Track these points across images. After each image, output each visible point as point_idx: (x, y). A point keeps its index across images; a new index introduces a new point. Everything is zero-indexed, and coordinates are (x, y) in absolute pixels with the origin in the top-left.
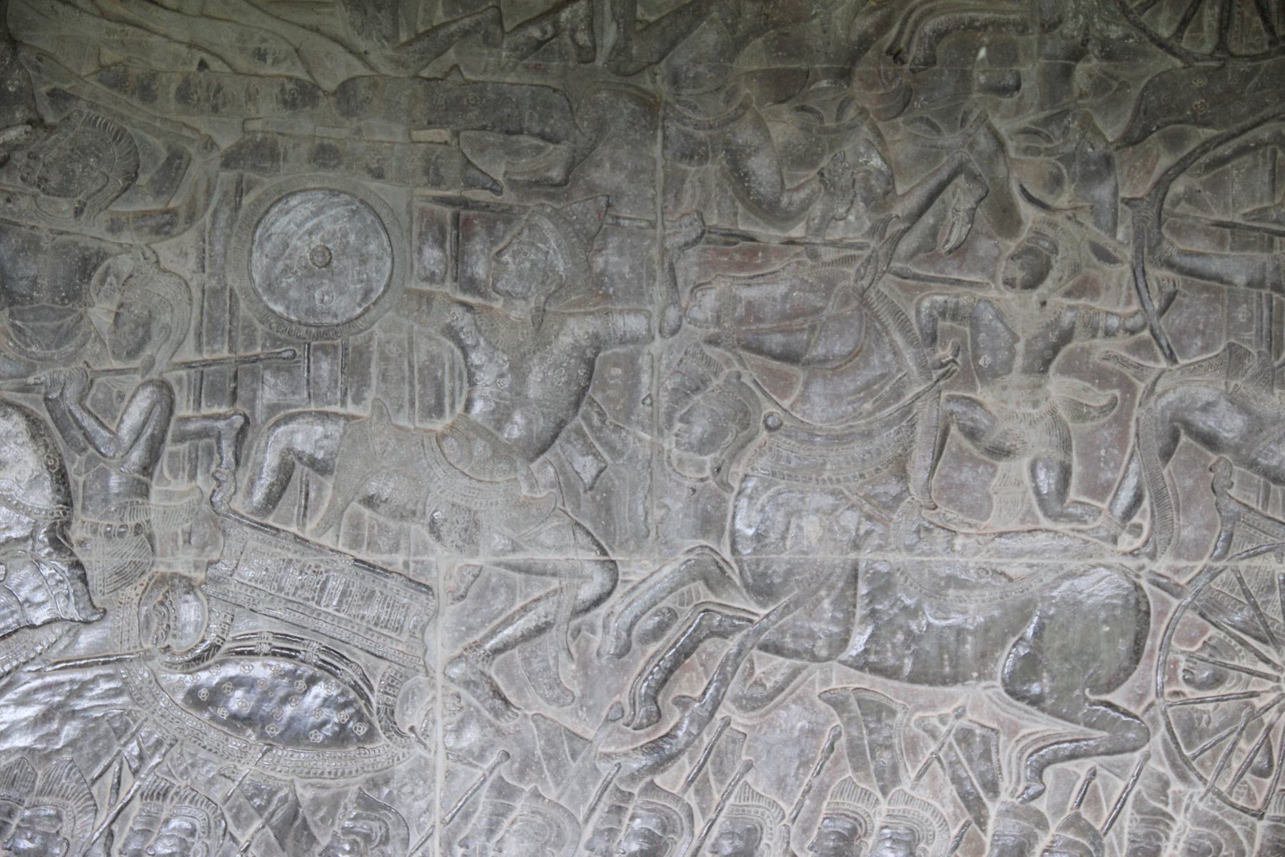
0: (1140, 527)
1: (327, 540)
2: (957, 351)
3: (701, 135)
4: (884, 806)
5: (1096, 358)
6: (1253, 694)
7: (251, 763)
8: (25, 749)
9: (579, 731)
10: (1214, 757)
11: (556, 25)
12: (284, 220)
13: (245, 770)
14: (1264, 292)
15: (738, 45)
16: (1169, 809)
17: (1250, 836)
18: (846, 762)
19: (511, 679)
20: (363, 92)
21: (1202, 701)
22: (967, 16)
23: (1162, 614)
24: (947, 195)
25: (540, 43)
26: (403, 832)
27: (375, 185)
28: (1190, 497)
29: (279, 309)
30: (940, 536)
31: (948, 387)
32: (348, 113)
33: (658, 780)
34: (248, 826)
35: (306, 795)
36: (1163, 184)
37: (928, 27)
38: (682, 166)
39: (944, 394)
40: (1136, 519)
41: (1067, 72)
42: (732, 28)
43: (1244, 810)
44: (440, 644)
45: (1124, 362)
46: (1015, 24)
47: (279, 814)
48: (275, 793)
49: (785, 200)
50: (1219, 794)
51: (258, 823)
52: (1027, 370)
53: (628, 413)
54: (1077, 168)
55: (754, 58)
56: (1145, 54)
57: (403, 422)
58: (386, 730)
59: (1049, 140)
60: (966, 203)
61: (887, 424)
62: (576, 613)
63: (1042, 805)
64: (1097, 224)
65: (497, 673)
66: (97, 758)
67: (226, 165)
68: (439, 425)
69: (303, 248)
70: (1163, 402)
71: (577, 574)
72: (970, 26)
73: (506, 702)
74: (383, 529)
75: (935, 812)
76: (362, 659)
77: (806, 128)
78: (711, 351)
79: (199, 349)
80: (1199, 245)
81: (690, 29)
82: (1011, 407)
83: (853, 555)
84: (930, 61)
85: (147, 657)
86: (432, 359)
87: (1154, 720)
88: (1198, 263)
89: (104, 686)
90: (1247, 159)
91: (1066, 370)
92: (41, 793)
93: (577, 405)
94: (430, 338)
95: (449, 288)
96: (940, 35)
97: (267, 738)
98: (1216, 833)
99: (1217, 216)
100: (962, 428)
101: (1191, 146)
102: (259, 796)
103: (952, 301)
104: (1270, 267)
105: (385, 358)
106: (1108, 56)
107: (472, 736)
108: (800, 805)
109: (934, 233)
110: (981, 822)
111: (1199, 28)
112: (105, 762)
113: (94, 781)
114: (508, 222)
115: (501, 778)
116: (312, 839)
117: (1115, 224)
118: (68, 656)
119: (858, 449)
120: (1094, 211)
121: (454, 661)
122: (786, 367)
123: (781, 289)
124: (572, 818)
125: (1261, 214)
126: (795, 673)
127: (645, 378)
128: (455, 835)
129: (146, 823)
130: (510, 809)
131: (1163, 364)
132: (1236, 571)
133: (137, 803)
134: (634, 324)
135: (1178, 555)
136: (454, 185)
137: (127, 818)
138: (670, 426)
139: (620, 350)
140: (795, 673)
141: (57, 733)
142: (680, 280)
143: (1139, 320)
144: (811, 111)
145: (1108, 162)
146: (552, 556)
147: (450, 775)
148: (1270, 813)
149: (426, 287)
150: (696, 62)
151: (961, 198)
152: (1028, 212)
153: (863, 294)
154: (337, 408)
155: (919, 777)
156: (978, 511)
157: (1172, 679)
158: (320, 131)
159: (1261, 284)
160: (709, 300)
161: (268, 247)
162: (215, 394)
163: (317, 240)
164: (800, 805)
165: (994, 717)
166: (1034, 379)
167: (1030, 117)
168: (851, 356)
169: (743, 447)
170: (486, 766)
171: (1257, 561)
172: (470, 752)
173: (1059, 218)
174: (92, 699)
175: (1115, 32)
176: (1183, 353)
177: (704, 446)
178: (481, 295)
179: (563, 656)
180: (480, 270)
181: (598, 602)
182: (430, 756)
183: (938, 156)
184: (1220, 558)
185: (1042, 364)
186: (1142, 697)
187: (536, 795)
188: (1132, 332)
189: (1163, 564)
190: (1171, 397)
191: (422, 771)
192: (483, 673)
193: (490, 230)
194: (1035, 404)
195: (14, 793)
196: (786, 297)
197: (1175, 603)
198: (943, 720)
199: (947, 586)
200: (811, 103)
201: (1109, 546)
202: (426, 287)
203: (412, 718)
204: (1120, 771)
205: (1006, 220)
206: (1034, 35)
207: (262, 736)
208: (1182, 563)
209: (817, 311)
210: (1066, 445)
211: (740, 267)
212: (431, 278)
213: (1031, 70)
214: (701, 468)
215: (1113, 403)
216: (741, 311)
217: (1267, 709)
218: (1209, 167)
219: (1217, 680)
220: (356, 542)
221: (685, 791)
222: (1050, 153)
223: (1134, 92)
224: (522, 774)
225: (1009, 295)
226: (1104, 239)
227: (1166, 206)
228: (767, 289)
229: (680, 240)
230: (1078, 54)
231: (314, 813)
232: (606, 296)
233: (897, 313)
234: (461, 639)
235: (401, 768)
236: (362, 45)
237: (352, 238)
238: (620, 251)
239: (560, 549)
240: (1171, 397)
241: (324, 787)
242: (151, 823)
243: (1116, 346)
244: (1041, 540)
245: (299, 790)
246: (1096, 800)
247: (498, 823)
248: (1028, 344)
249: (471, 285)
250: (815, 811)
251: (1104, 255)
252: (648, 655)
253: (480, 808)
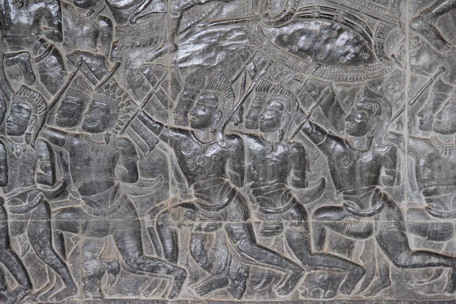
7: (311, 74)
8: (199, 65)
13: (307, 77)
19: (446, 29)
26: (388, 109)
34: (309, 105)
35: (338, 90)
47: (325, 99)
48: (323, 89)
51: (314, 104)
58: (379, 56)
65: (438, 26)
66: (234, 70)
73: (444, 41)
76: (366, 19)
85: (257, 19)
89: (236, 34)
92: (208, 87)
97: (318, 61)
102: (314, 91)
107: (425, 59)
112: (237, 73)
113: (233, 82)
115: (440, 81)
116: (342, 112)
118: (218, 19)
121: (415, 20)
128: (416, 110)
129: (259, 103)
130: (446, 97)
133: (254, 94)
137: (249, 101)
141: (214, 58)
147: (413, 79)
170: (432, 75)
172: (424, 67)
174: (230, 41)
182: (403, 70)
191: (398, 77)
192: (431, 26)
195: (194, 87)
203: (393, 50)
207: (315, 60)
231: (342, 99)
234: (419, 7)
235: (387, 76)
241: (347, 86)
242: (261, 103)
245: (335, 88)
247: (439, 104)
253: (429, 96)
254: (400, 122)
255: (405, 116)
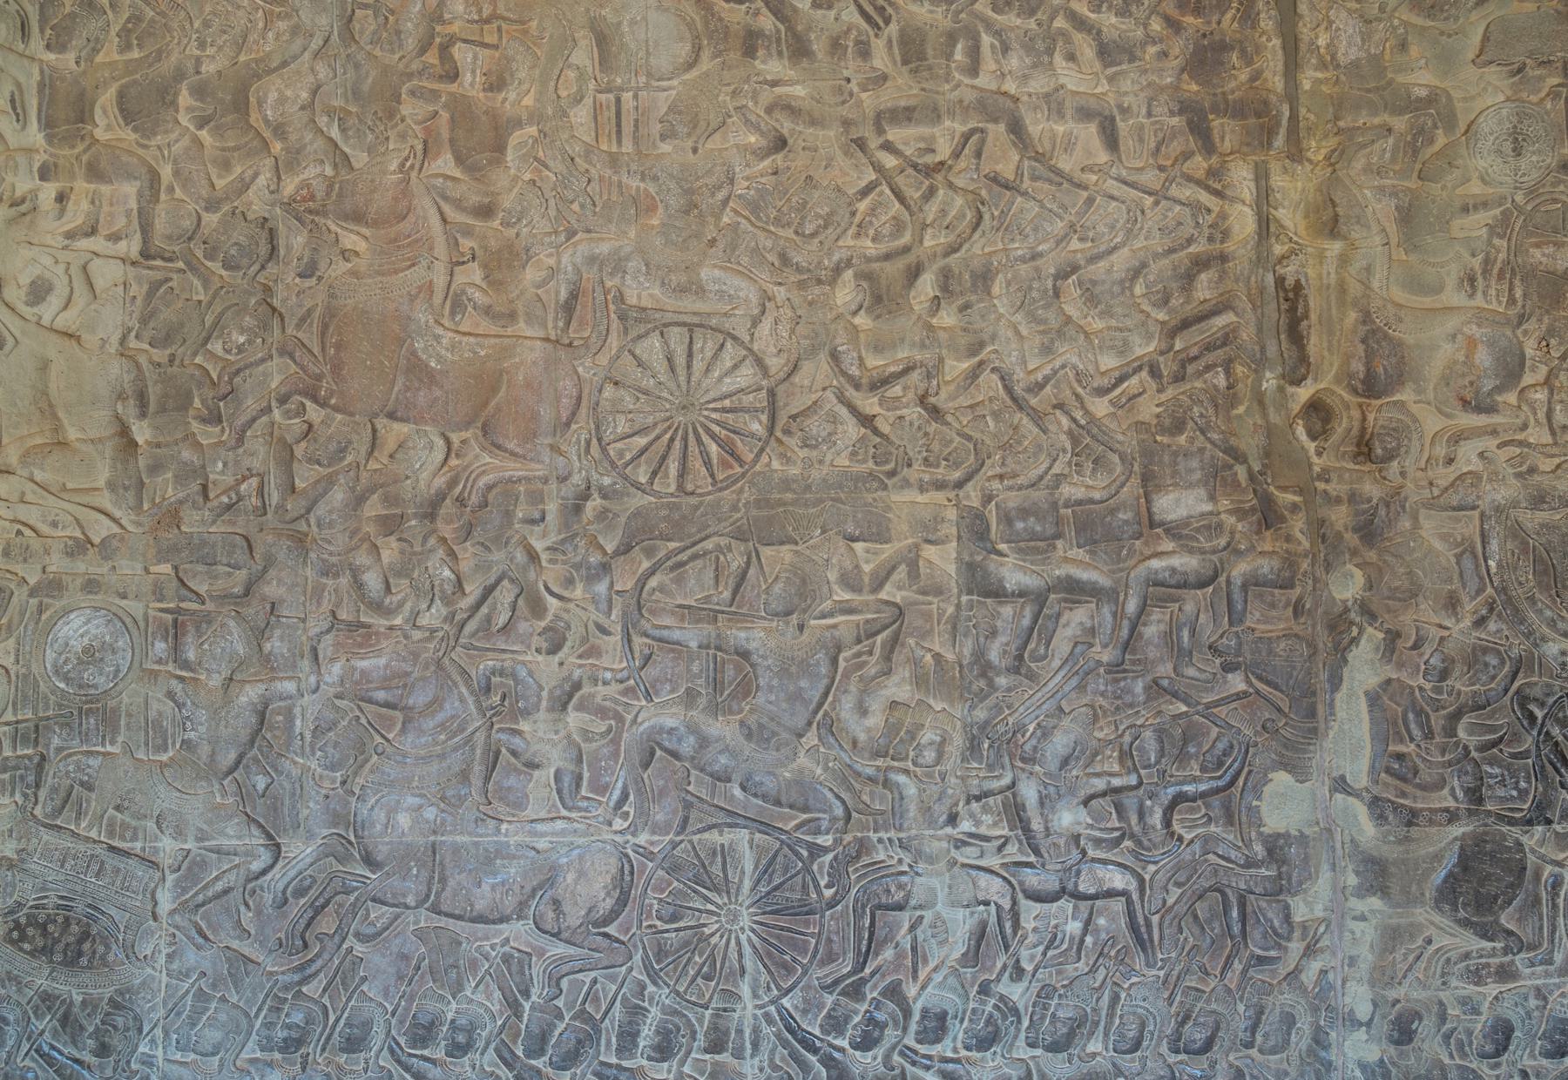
0: (627, 813)
1: (93, 834)
2: (504, 697)
3: (334, 559)
4: (454, 1005)
5: (598, 699)
6: (704, 925)
9: (253, 957)
10: (675, 969)
11: (237, 494)
12: (66, 628)
14: (711, 652)
15: (360, 500)
16: (646, 1004)
17: (700, 1020)
18: (428, 977)
20: (115, 543)
21: (667, 931)
22: (507, 474)
23: (642, 872)
24: (496, 593)
25: (229, 507)
27: (123, 603)
28: (663, 793)
29: (62, 685)
30: (492, 823)
31: (500, 722)
32: (106, 558)
33: (304, 989)
35: (78, 999)
36: (642, 582)
37: (481, 483)
38: (324, 580)
39: (496, 727)
40: (625, 808)
41: (578, 509)
42: (353, 489)
43: (694, 1004)
44: (166, 901)
45: (616, 702)
46: (539, 478)
49: (387, 601)
50: (678, 993)
52: (551, 709)
53: (288, 745)
54: (584, 572)
55: (374, 507)
56: (628, 495)
57: (141, 756)
59: (564, 553)
60: (510, 598)
61: (455, 749)
62: (249, 880)
63: (560, 1003)
64: (597, 609)
67: (31, 595)
68: (164, 758)
69: (77, 645)
70: (641, 729)
71: (250, 854)
72: (510, 480)
74: (128, 826)
75: (487, 1009)
77: (402, 552)
78: (338, 702)
79: (15, 714)
80: (667, 621)
81: (325, 493)
82: (540, 734)
83: (432, 838)
84: (484, 504)
86: (160, 714)
87: (635, 946)
88: (665, 633)
90: (699, 563)
91: (580, 707)
93: (252, 742)
94: (159, 700)
95: (170, 667)
96: (490, 488)
98: (676, 1020)
99: (680, 601)
100: (508, 749)
101: (661, 554)
102: (47, 998)
103: (498, 664)
104: (713, 634)
105: (129, 715)
106: (604, 497)
108: (398, 1005)
109: (488, 619)
110: (518, 1014)
111: (666, 476)
114: (209, 623)
116: (82, 1028)
117: (610, 609)
119: (435, 767)
120: (594, 601)
122: (391, 712)
123: (383, 661)
124: (247, 1015)
125: (707, 599)
126: (397, 917)
127: (298, 723)
130: (207, 1009)
131: (644, 703)
132: (691, 842)
134: (289, 687)
135: (654, 833)
136: (171, 601)
138: (313, 754)
139: (282, 704)
140: (397, 917)
142: (321, 656)
143: (625, 674)
144: (405, 540)
145: (605, 568)
146: (235, 842)
148: (713, 1005)
149: (156, 667)
150: (330, 512)
151: (505, 594)
152: (553, 603)
153: (439, 662)
154: (99, 748)
155: (477, 986)
156: (519, 805)
157: (649, 916)
158: (91, 570)
159: (708, 647)
160: (337, 669)
161: (56, 646)
162: (25, 740)
163: (86, 641)
164: (398, 1005)
165: (529, 945)
166: (556, 715)
167: (553, 539)
168: (430, 705)
169: (362, 766)
171: (706, 835)
173: (571, 606)
175: (607, 481)
176: (657, 694)
177: (333, 767)
178: (192, 671)
179: (242, 908)
180: (191, 655)
181: (264, 872)
183: (490, 568)
184: (678, 834)
185: (561, 704)
186: (628, 930)
187: (223, 999)
188: (621, 682)
189: (643, 838)
190: (646, 725)
193: (198, 629)
194: (556, 732)
196: (386, 666)
197: (651, 865)
198: (493, 947)
199: (496, 857)
200: (405, 536)
201: (606, 828)
202: (156, 667)
204: (612, 979)
205: (538, 609)
206: (553, 486)
208: (656, 838)
209: (407, 674)
210: (580, 760)
211: (360, 646)
212: (160, 662)
213: (552, 508)
214: (334, 782)
215: (609, 730)
216: (357, 676)
217: (713, 935)
218: (672, 569)
219: (674, 918)
220: (111, 834)
221: (321, 996)
222: (564, 562)
223: (623, 520)
224: (214, 986)
225: (540, 658)
226: (602, 620)
227: (644, 595)
228: (373, 661)
229: (317, 630)
230: (585, 496)
232: (272, 669)
233: (464, 672)
234: (178, 897)
236: (118, 514)
237: (107, 638)
238: (282, 639)
239: (239, 838)
240: (646, 725)
243: (614, 689)
244: (560, 825)
246: (596, 1000)
248: (551, 692)
249: (186, 665)
250: (407, 1009)
251: (604, 631)
252: (297, 907)
254: (153, 1041)
255: (159, 1032)
